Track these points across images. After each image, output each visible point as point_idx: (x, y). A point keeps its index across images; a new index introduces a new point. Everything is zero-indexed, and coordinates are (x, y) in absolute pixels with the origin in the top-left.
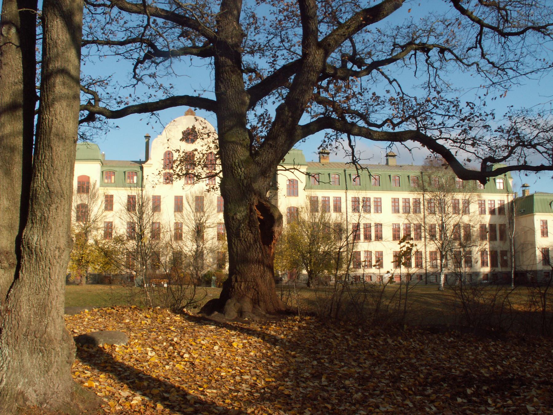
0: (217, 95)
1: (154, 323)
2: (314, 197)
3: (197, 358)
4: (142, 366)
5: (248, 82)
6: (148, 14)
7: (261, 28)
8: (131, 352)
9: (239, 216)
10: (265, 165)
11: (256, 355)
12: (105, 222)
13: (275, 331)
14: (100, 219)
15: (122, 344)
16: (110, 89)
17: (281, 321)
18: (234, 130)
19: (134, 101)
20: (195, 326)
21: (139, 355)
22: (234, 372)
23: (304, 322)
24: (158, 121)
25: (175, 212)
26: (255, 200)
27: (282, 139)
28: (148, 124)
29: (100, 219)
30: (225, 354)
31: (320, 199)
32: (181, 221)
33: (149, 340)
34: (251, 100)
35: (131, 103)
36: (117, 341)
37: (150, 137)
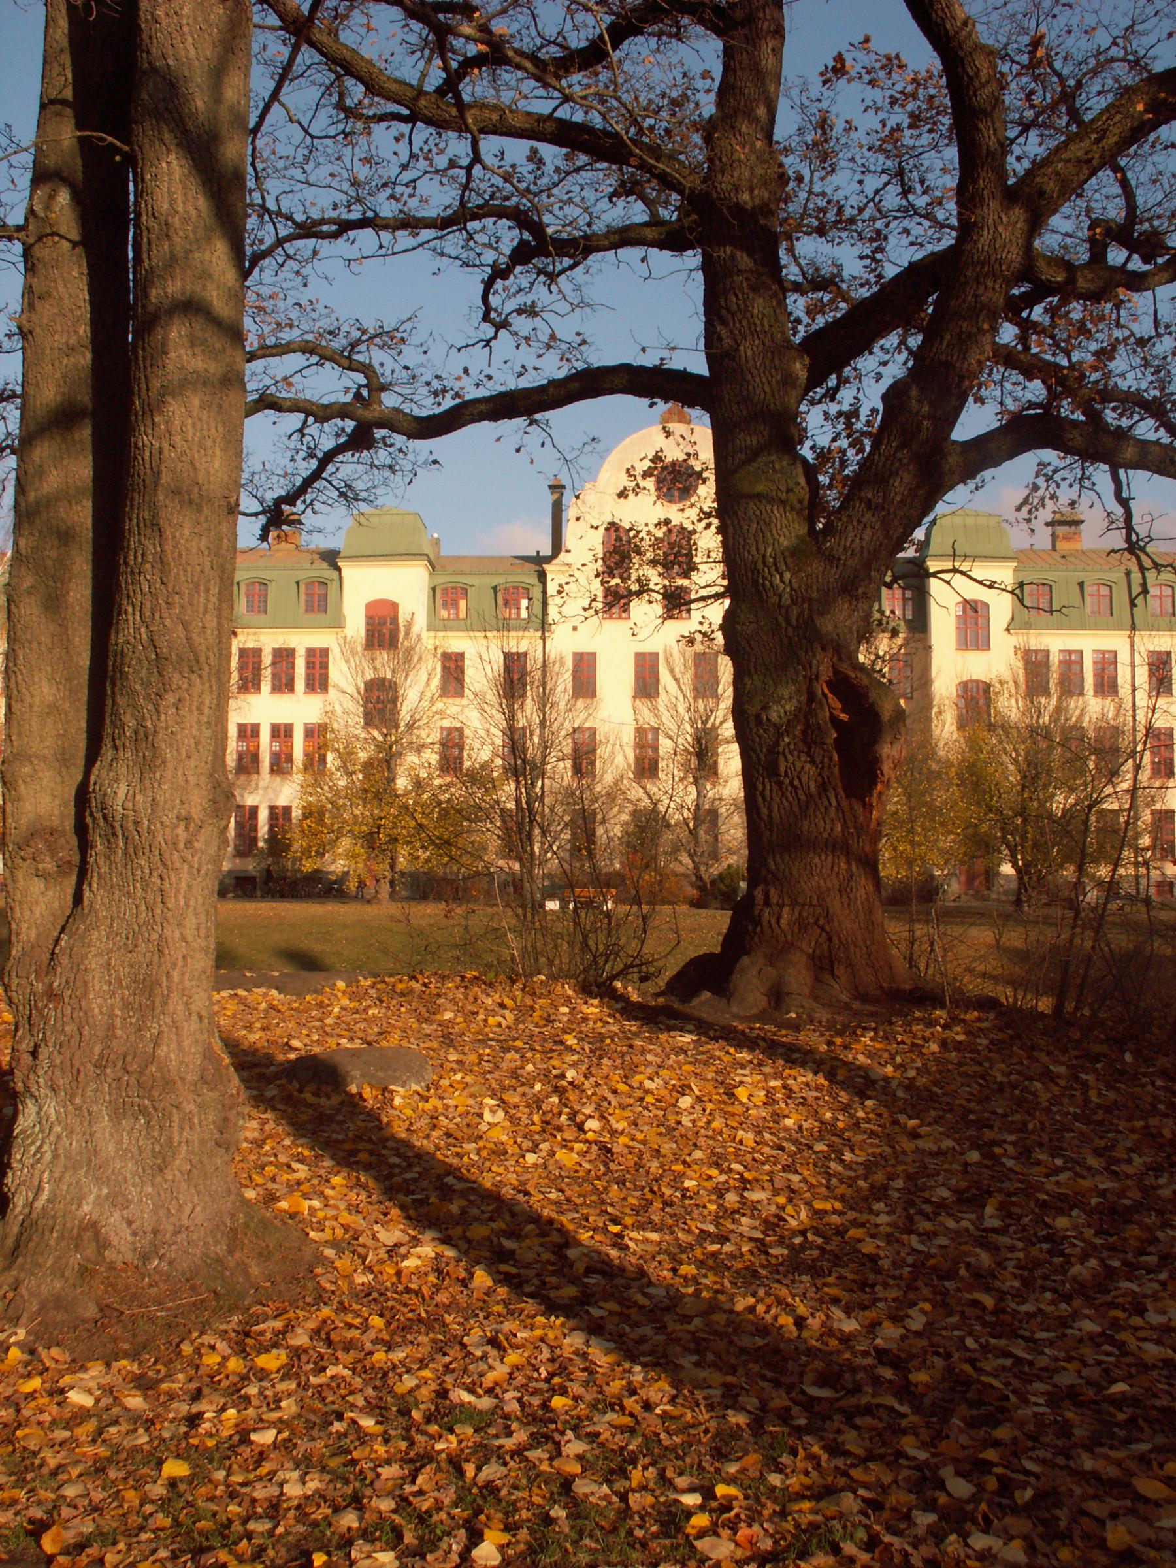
0: (710, 359)
1: (523, 1022)
2: (1036, 652)
3: (622, 1133)
4: (457, 1154)
5: (806, 320)
6: (474, 129)
7: (841, 155)
8: (436, 1109)
9: (775, 713)
10: (853, 562)
11: (800, 1127)
12: (442, 728)
13: (870, 1055)
14: (424, 721)
15: (415, 1087)
16: (410, 356)
17: (891, 1023)
18: (763, 459)
19: (477, 385)
20: (636, 1034)
21: (458, 1120)
22: (723, 1178)
23: (958, 1029)
24: (548, 442)
25: (635, 697)
26: (824, 666)
27: (900, 485)
28: (518, 451)
29: (424, 721)
30: (709, 1122)
31: (1055, 658)
32: (654, 723)
33: (497, 1075)
34: (810, 370)
35: (472, 394)
36: (398, 1078)
37: (564, 487)
